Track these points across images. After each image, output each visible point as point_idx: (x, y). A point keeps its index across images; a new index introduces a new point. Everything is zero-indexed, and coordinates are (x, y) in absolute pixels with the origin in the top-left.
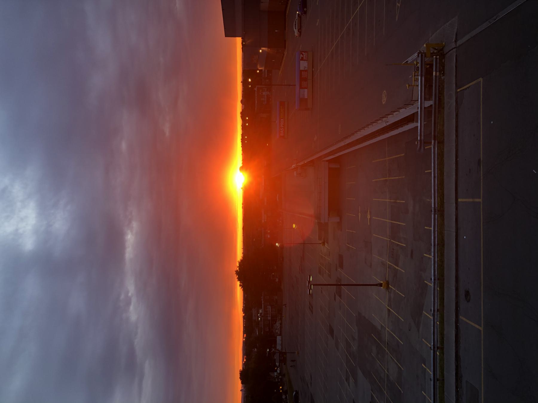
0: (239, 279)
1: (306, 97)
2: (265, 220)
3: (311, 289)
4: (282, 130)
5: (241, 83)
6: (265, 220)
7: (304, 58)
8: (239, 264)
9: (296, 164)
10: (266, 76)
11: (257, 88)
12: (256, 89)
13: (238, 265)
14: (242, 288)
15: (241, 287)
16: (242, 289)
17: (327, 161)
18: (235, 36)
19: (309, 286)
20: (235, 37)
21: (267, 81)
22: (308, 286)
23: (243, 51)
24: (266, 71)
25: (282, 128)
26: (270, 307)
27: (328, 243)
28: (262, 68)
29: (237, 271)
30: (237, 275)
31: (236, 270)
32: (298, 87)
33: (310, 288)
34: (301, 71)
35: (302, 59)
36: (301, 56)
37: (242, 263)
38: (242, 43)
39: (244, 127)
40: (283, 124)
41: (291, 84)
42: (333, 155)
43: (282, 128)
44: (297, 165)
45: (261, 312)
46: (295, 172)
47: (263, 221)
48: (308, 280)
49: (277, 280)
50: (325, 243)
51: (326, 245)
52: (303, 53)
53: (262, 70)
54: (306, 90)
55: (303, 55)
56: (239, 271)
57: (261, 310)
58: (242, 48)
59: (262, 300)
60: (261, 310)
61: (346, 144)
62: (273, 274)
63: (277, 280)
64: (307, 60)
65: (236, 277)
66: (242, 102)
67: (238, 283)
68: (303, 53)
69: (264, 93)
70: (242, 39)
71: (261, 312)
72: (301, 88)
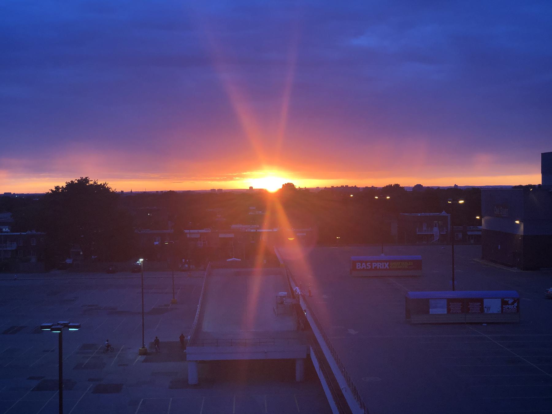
0: (70, 185)
1: (432, 311)
2: (188, 236)
3: (52, 330)
4: (367, 266)
5: (453, 185)
6: (188, 236)
7: (507, 306)
8: (101, 184)
9: (301, 294)
10: (469, 233)
11: (447, 215)
12: (444, 213)
13: (99, 183)
14: (52, 190)
15: (54, 190)
16: (50, 192)
17: (309, 355)
18: (545, 173)
19: (59, 326)
20: (542, 173)
21: (460, 236)
22: (58, 324)
23: (515, 187)
24: (480, 233)
25: (371, 265)
26: (14, 246)
27: (145, 361)
28: (484, 226)
29: (86, 180)
30: (78, 180)
31: (90, 180)
32: (451, 294)
33: (53, 327)
34: (481, 301)
35: (504, 303)
36: (511, 301)
37: (102, 190)
38: (530, 186)
39: (371, 191)
40: (378, 268)
41: (455, 282)
42: (321, 367)
43: (371, 265)
44: (300, 296)
45: (4, 230)
46: (286, 293)
47: (186, 231)
48: (71, 324)
49: (69, 261)
50: (145, 356)
51: (141, 358)
52: (516, 304)
53: (481, 225)
54: (445, 311)
55: (513, 304)
56: (88, 184)
57: (7, 229)
58: (520, 187)
59: (29, 232)
60: (7, 229)
61: (343, 392)
62: (81, 253)
63: (69, 261)
64: (502, 311)
65: (74, 178)
66: (419, 187)
67: (62, 184)
68: (516, 304)
69: (436, 229)
70: (539, 185)
71: (4, 230)
72: (450, 301)
